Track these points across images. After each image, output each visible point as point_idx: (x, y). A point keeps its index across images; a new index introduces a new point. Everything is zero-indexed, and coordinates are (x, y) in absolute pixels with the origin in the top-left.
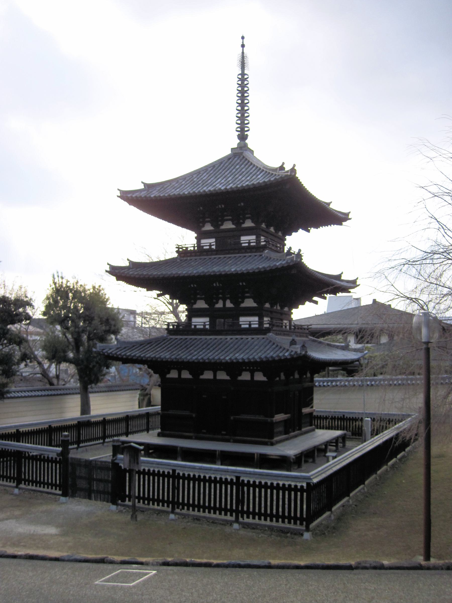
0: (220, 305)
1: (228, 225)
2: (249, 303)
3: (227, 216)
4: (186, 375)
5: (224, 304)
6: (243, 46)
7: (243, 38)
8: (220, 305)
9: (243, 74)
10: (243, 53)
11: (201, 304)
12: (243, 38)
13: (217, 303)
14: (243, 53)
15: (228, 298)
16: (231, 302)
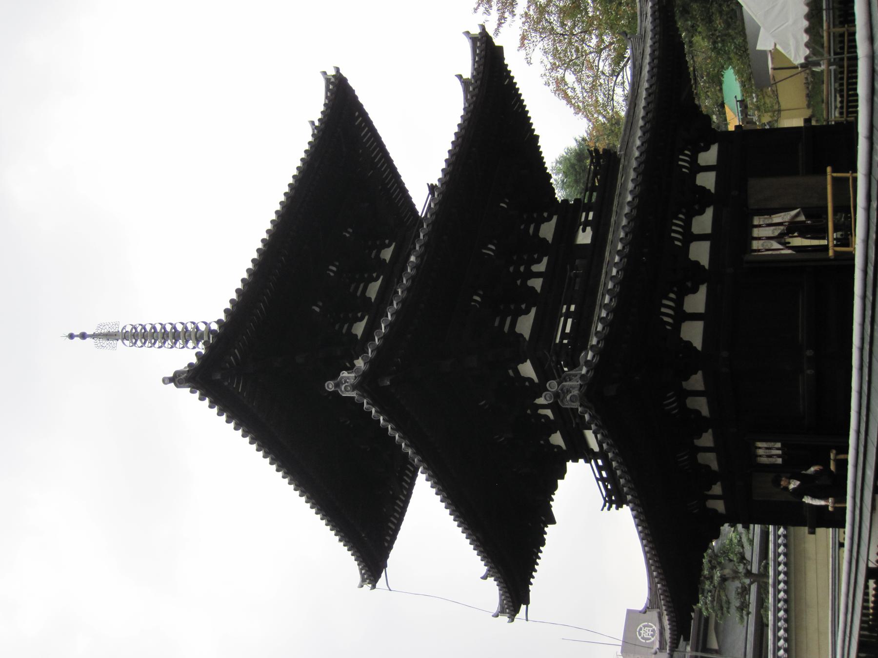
0: (537, 284)
1: (373, 290)
2: (548, 231)
3: (357, 288)
4: (697, 302)
5: (538, 275)
6: (83, 336)
7: (71, 336)
8: (537, 284)
9: (125, 336)
10: (94, 336)
11: (525, 325)
12: (71, 336)
13: (533, 288)
14: (94, 336)
15: (528, 269)
16: (539, 261)
